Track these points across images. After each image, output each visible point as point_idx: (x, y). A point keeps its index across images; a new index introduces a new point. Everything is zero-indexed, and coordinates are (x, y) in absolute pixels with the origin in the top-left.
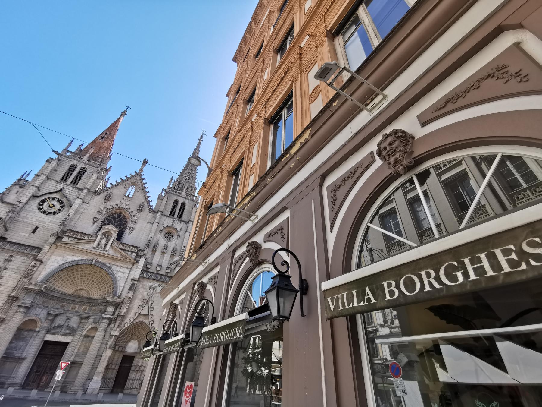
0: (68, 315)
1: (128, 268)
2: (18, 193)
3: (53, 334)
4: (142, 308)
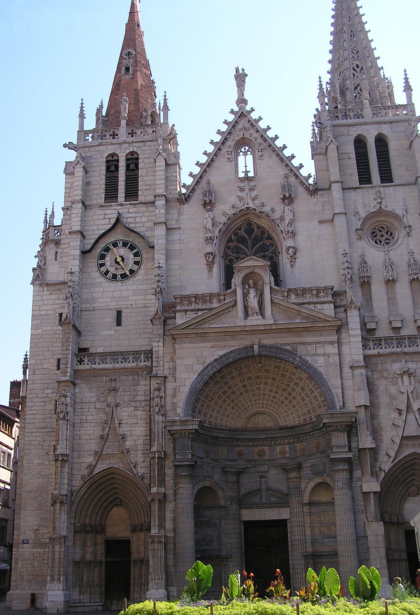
0: (258, 469)
1: (332, 343)
3: (251, 507)
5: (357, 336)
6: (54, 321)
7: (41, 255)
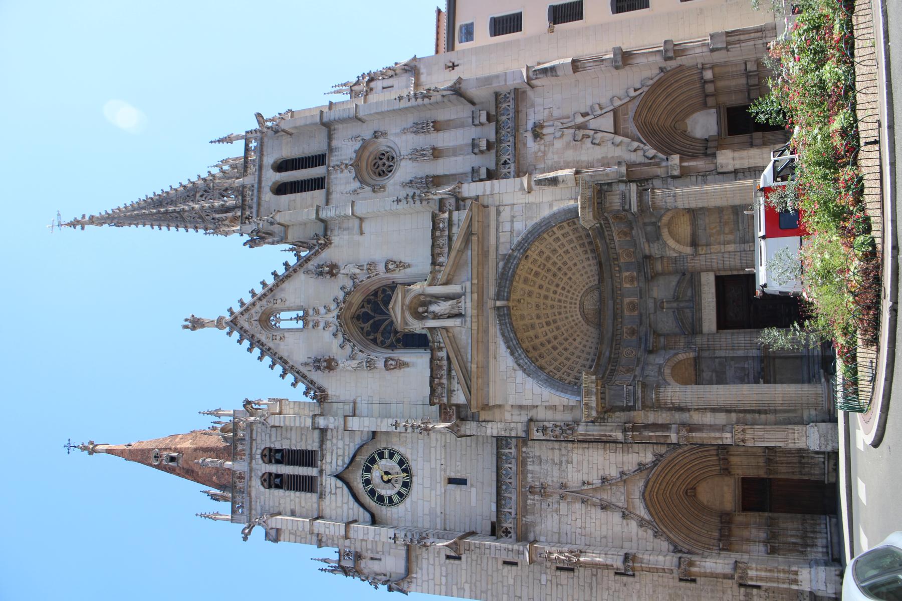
0: (652, 311)
1: (498, 213)
2: (378, 556)
4: (600, 135)
6: (455, 566)
7: (374, 580)
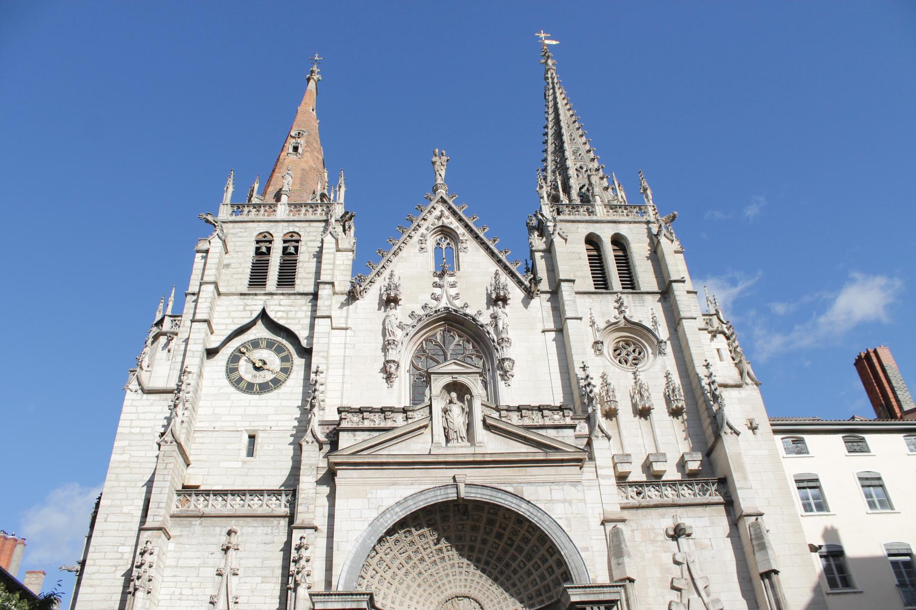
5: (606, 477)
